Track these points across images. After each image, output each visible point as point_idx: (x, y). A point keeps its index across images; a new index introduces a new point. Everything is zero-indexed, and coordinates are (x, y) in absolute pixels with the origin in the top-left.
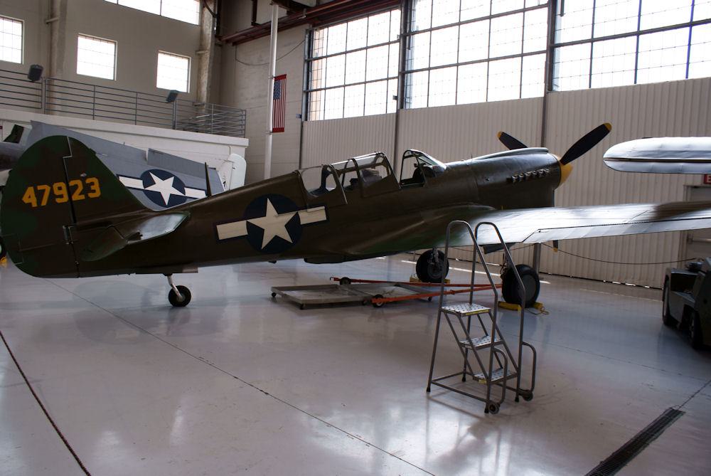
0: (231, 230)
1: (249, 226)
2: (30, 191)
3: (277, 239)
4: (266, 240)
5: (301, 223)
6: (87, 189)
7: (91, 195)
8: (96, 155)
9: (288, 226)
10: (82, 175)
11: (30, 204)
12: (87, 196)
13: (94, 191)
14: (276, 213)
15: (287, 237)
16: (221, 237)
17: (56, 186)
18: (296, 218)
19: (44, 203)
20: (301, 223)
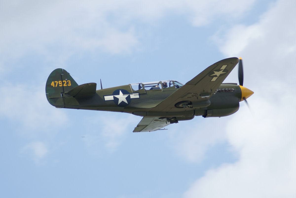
1: (114, 97)
2: (53, 83)
3: (123, 102)
4: (120, 102)
6: (67, 83)
7: (68, 85)
9: (127, 98)
10: (66, 79)
11: (53, 86)
12: (67, 85)
13: (69, 84)
15: (126, 102)
16: (106, 100)
17: (59, 82)
18: (129, 96)
19: (56, 86)
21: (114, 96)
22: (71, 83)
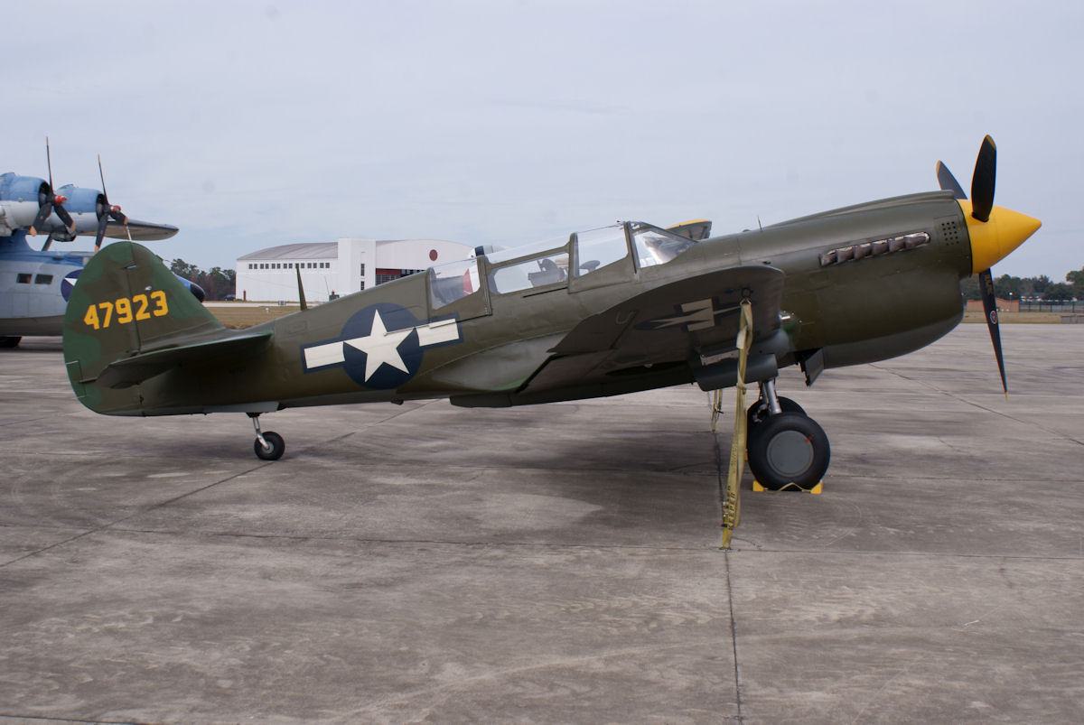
0: (322, 355)
1: (348, 350)
2: (92, 309)
3: (385, 369)
4: (371, 369)
5: (421, 344)
6: (153, 305)
7: (157, 313)
8: (164, 262)
10: (147, 289)
12: (152, 314)
13: (160, 308)
14: (385, 331)
15: (400, 365)
16: (310, 364)
17: (119, 302)
18: (414, 338)
19: (106, 324)
20: (421, 344)
21: (348, 342)
22: (168, 301)
